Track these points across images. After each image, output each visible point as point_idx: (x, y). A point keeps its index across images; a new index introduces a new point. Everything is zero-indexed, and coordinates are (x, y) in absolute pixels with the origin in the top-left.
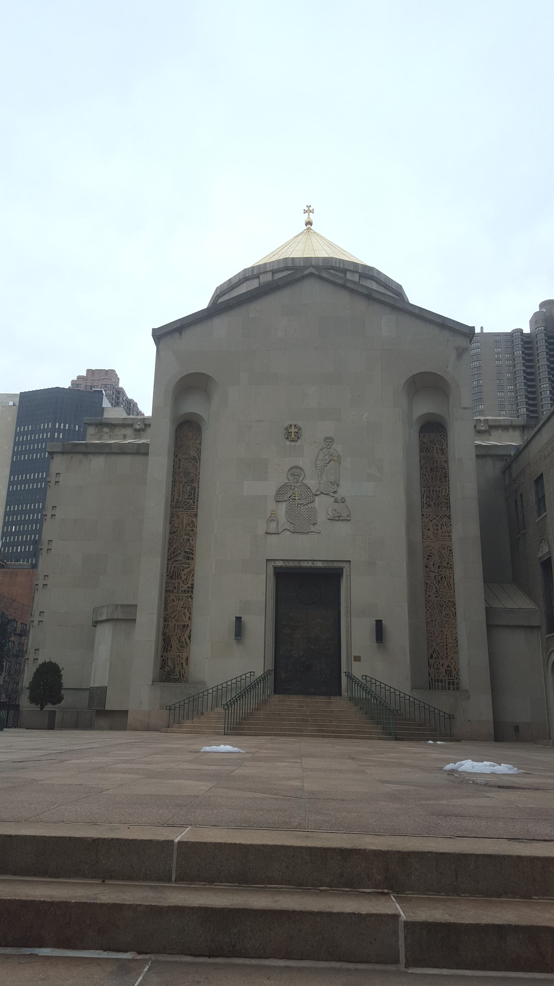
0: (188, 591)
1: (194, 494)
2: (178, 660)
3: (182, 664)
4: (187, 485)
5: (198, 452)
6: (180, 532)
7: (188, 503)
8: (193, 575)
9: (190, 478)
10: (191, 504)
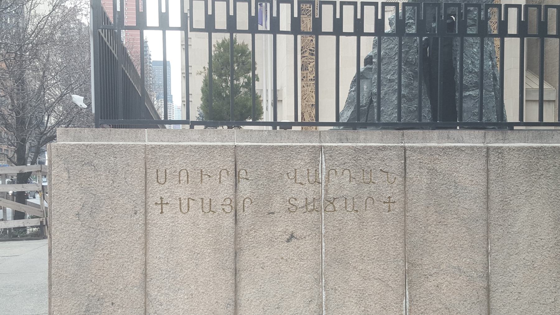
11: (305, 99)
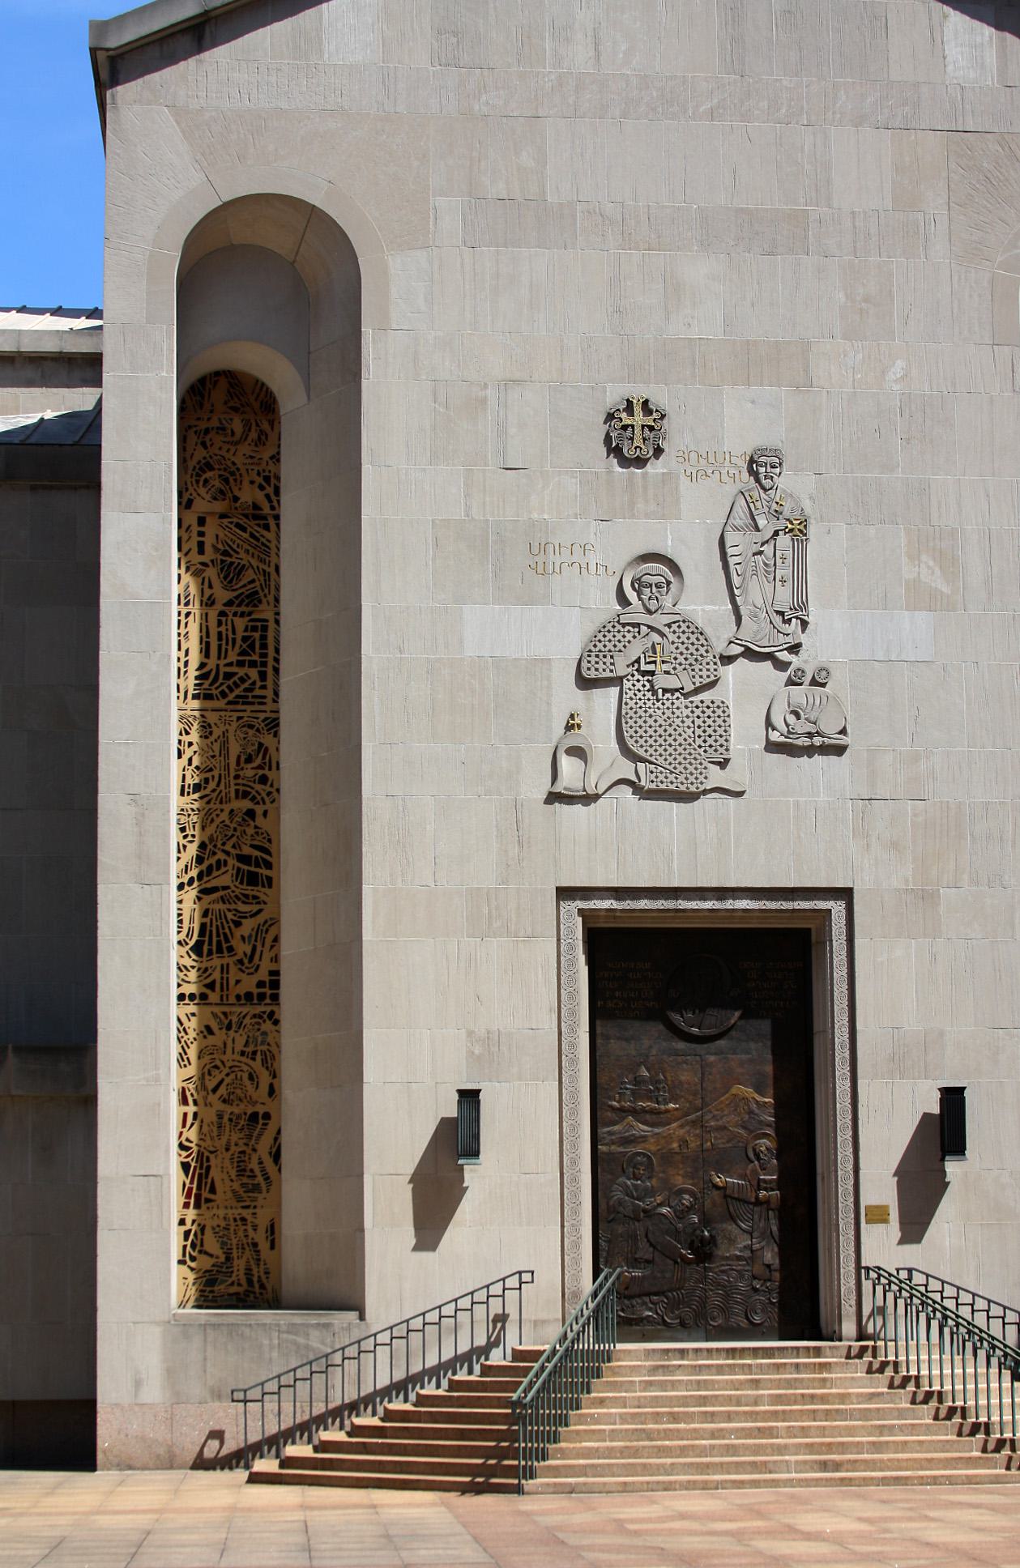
0: (262, 997)
1: (264, 646)
2: (241, 1234)
3: (255, 1245)
4: (235, 614)
5: (270, 490)
6: (218, 785)
7: (242, 680)
8: (276, 939)
9: (244, 586)
10: (254, 683)
11: (215, 1090)
